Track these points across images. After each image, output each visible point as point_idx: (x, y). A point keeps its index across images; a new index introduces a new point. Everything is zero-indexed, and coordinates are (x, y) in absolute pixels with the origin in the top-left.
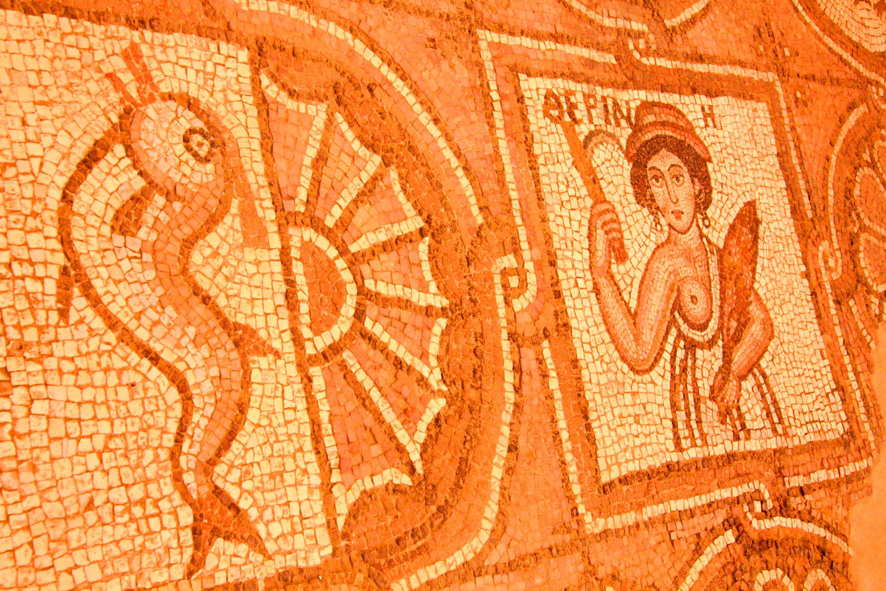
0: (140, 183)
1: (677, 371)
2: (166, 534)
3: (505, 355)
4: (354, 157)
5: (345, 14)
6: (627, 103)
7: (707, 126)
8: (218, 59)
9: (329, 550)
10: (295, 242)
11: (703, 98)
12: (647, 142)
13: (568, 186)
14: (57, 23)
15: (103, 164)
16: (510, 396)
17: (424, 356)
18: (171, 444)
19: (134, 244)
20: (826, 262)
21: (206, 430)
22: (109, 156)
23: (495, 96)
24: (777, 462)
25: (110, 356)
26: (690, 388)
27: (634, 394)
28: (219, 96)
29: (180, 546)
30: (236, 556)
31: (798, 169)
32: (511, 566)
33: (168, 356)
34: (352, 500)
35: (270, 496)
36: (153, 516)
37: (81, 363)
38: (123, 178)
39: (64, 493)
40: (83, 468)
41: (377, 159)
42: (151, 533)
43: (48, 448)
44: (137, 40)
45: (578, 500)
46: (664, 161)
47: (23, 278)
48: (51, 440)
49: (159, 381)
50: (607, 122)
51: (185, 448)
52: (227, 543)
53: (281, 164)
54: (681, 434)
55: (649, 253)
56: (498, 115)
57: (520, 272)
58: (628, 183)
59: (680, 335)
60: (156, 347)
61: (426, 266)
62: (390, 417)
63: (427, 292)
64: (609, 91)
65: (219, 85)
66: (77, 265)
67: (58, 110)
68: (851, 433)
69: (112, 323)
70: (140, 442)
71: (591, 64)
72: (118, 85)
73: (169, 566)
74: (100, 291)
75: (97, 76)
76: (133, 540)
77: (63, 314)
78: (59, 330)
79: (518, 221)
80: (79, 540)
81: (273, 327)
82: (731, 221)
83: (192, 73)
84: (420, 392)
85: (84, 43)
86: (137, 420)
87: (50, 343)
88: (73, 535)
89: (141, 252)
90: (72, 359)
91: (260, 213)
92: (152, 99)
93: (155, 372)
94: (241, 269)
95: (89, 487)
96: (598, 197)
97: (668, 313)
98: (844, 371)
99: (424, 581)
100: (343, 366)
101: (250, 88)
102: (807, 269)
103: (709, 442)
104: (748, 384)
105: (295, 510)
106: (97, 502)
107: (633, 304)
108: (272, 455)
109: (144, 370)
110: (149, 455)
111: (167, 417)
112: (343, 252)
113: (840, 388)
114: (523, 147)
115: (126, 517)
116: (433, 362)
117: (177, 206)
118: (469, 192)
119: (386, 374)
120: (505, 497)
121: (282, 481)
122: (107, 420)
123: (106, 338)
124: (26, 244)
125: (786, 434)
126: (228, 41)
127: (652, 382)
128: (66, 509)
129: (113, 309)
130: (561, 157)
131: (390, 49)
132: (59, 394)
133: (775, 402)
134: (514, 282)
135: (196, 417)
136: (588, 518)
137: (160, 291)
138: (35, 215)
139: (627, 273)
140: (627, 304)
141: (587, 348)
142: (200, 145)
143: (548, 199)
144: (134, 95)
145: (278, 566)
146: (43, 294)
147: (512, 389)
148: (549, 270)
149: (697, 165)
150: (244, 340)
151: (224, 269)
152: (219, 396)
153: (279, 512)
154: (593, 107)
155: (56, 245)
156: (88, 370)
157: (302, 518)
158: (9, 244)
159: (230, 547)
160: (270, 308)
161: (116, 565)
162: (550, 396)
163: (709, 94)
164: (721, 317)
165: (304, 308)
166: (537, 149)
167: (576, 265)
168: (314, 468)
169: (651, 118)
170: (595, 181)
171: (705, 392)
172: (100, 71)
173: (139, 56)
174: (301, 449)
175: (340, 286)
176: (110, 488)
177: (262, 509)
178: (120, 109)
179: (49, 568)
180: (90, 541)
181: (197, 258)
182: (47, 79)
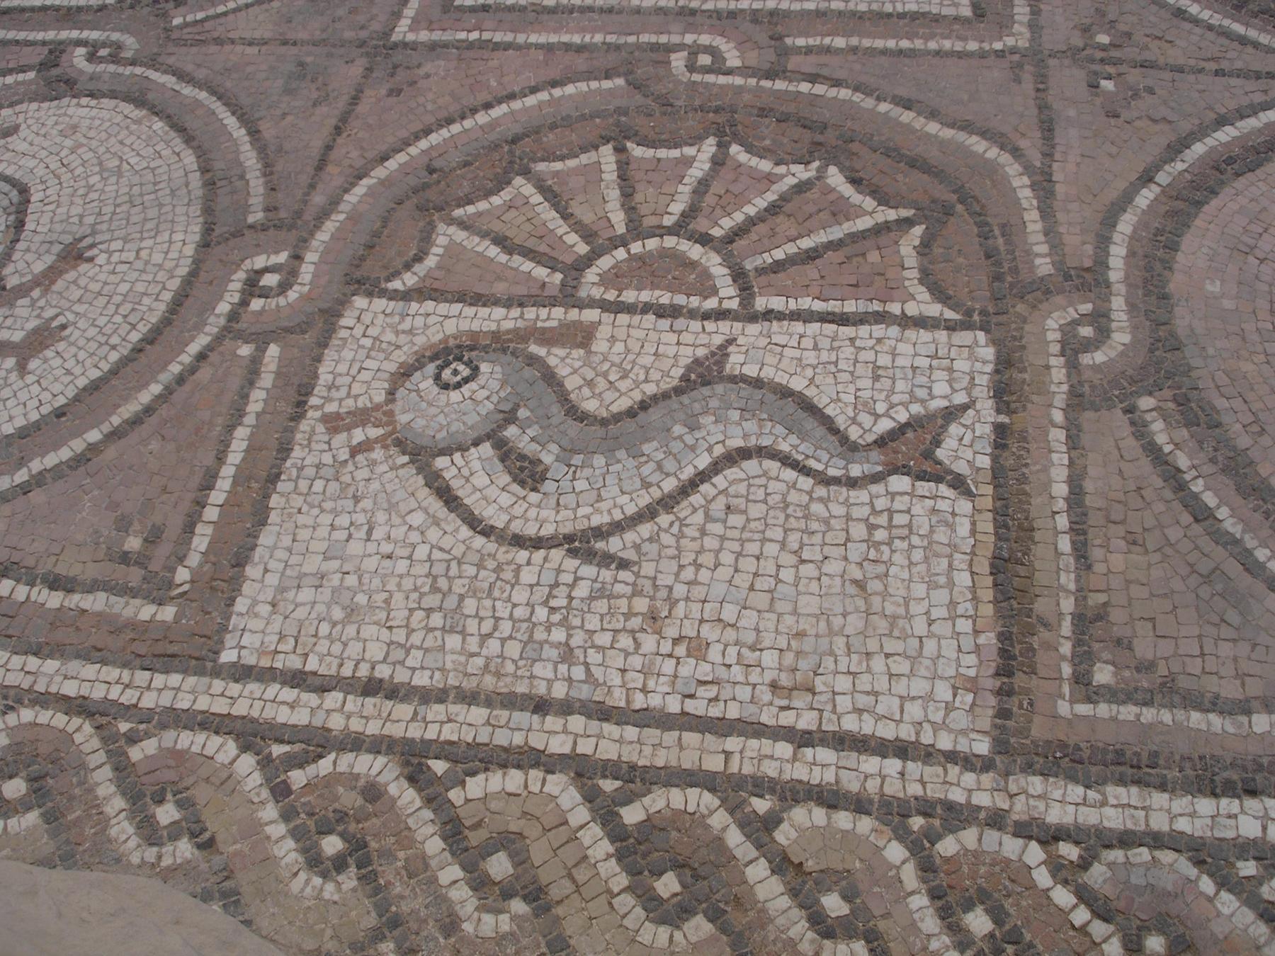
0: (486, 449)
2: (917, 510)
5: (338, 181)
8: (358, 331)
9: (981, 335)
10: (597, 293)
14: (282, 495)
15: (455, 484)
16: (844, 93)
17: (770, 179)
18: (810, 481)
19: (558, 470)
22: (447, 475)
23: (474, 36)
25: (687, 525)
28: (403, 339)
29: (935, 497)
30: (961, 439)
33: (703, 462)
34: (926, 296)
35: (900, 385)
36: (891, 519)
37: (688, 558)
38: (476, 465)
40: (815, 584)
41: (519, 181)
42: (909, 526)
43: (780, 615)
44: (318, 414)
45: (986, 46)
47: (570, 598)
49: (731, 478)
51: (820, 467)
52: (943, 445)
53: (500, 289)
56: (498, 37)
57: (695, 50)
60: (688, 473)
61: (662, 153)
62: (836, 233)
63: (694, 158)
65: (389, 336)
66: (569, 538)
67: (381, 517)
69: (648, 514)
70: (800, 515)
73: (954, 514)
74: (606, 519)
75: (350, 467)
76: (914, 547)
77: (624, 564)
78: (642, 573)
81: (697, 340)
84: (813, 194)
85: (310, 472)
86: (771, 513)
87: (655, 586)
88: (890, 609)
89: (569, 466)
90: (681, 567)
91: (554, 324)
92: (391, 414)
93: (719, 480)
94: (617, 360)
95: (838, 581)
99: (1041, 238)
100: (761, 271)
101: (401, 303)
105: (923, 362)
106: (858, 575)
108: (852, 373)
109: (713, 492)
110: (817, 508)
111: (777, 479)
112: (623, 242)
114: (545, 17)
115: (884, 548)
116: (782, 169)
117: (523, 413)
118: (583, 86)
119: (783, 224)
120: (967, 127)
122: (762, 545)
123: (665, 525)
124: (531, 586)
126: (340, 316)
128: (857, 611)
129: (631, 510)
131: (391, 139)
132: (719, 590)
134: (705, 60)
135: (784, 447)
136: (1010, 41)
137: (621, 454)
138: (498, 569)
142: (455, 372)
144: (380, 431)
145: (985, 395)
146: (595, 581)
147: (835, 89)
148: (699, 19)
150: (705, 374)
151: (612, 378)
152: (765, 416)
153: (922, 380)
155: (539, 555)
156: (698, 553)
157: (935, 356)
158: (527, 604)
159: (949, 443)
160: (673, 338)
161: (938, 571)
162: (854, 50)
165: (680, 300)
168: (878, 330)
172: (346, 461)
174: (852, 340)
175: (664, 253)
176: (846, 559)
177: (913, 399)
178: (393, 450)
179: (921, 641)
180: (903, 592)
181: (591, 406)
182: (344, 520)
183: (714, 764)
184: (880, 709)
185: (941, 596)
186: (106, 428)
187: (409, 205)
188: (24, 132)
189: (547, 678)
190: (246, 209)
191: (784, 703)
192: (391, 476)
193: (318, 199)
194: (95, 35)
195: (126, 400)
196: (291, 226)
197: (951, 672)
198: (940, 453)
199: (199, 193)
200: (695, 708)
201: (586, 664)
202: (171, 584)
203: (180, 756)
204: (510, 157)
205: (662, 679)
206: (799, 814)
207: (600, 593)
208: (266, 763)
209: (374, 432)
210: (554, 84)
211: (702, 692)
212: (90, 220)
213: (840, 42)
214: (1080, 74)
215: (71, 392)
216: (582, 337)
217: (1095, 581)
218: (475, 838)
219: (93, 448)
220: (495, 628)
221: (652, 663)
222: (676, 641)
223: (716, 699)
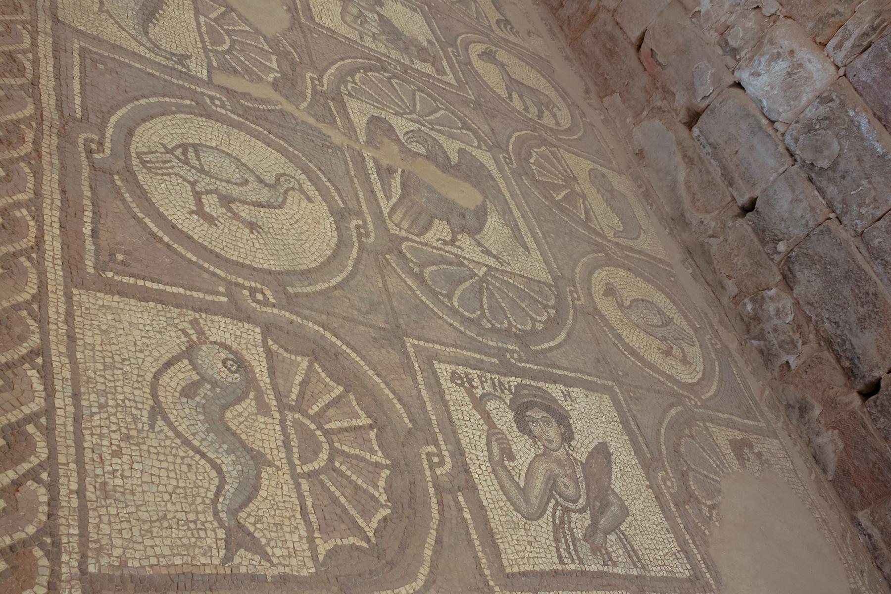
0: (196, 377)
2: (209, 541)
4: (326, 385)
6: (509, 383)
7: (566, 400)
8: (242, 329)
11: (562, 387)
17: (376, 486)
18: (212, 497)
19: (193, 403)
21: (233, 494)
23: (417, 369)
28: (244, 346)
29: (218, 548)
33: (211, 455)
35: (274, 535)
39: (149, 509)
41: (341, 388)
42: (200, 537)
46: (537, 414)
47: (131, 407)
48: (143, 482)
50: (495, 390)
51: (221, 500)
55: (531, 459)
64: (496, 376)
65: (243, 341)
66: (160, 406)
69: (178, 435)
71: (482, 361)
72: (186, 334)
73: (211, 556)
74: (173, 420)
77: (152, 426)
79: (437, 430)
80: (158, 533)
83: (228, 335)
87: (143, 438)
88: (155, 530)
90: (156, 447)
92: (205, 343)
93: (203, 462)
103: (585, 562)
106: (169, 517)
110: (199, 500)
111: (210, 484)
115: (185, 527)
116: (382, 491)
121: (282, 528)
128: (151, 517)
129: (180, 429)
130: (464, 403)
131: (348, 339)
134: (436, 460)
137: (206, 425)
138: (138, 382)
139: (516, 467)
142: (232, 365)
143: (457, 422)
144: (195, 339)
149: (562, 419)
150: (258, 459)
153: (280, 544)
154: (486, 382)
159: (249, 556)
160: (273, 445)
166: (447, 397)
168: (302, 527)
169: (526, 392)
170: (489, 417)
171: (579, 534)
173: (198, 324)
174: (294, 516)
176: (176, 511)
181: (229, 415)
182: (148, 328)
183: (61, 459)
184: (102, 526)
185: (167, 551)
186: (171, 243)
187: (314, 346)
188: (310, 205)
189: (89, 400)
190: (293, 286)
191: (97, 486)
192: (174, 343)
193: (307, 312)
194: (371, 227)
195: (186, 249)
196: (290, 302)
197: (128, 556)
199: (297, 269)
200: (88, 453)
201: (100, 413)
202: (104, 271)
203: (25, 273)
204: (350, 381)
205: (99, 441)
206: (43, 490)
207: (135, 419)
208: (28, 303)
209: (194, 337)
210: (400, 400)
211: (96, 457)
212: (271, 231)
215: (185, 230)
216: (263, 409)
218: (9, 373)
219: (160, 240)
220: (110, 381)
221: (107, 437)
222: (119, 446)
223: (94, 461)
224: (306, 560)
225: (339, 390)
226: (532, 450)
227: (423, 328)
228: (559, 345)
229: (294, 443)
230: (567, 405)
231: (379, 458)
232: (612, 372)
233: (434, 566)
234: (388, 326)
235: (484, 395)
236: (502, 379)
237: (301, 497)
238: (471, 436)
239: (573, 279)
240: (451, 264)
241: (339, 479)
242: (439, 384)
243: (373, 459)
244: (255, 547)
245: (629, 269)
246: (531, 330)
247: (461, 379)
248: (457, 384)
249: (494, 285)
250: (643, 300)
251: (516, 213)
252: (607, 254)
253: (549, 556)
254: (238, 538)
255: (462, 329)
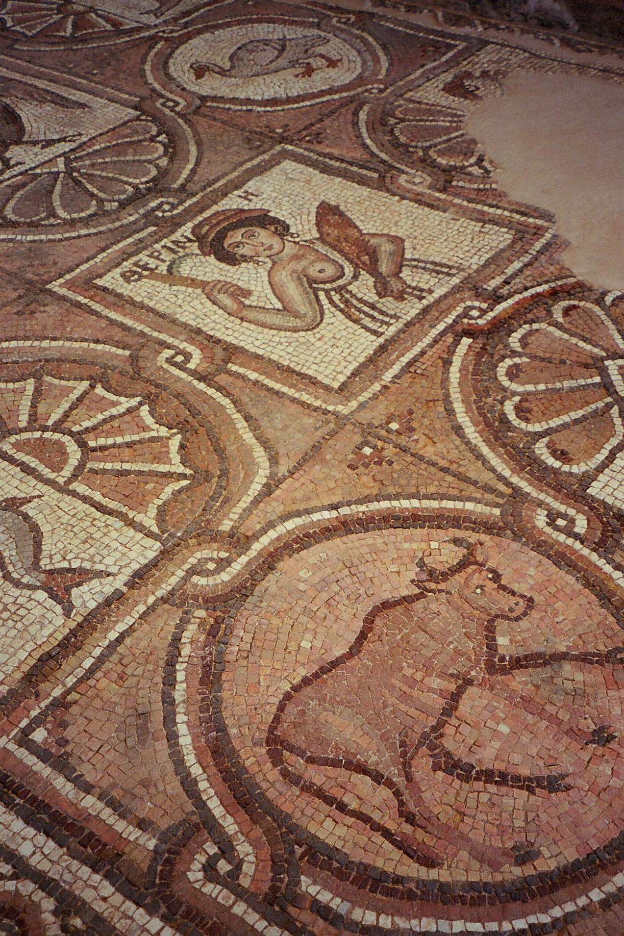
1: (342, 306)
3: (205, 390)
7: (250, 200)
11: (237, 193)
12: (213, 239)
13: (176, 296)
20: (414, 183)
23: (85, 301)
24: (473, 285)
26: (360, 306)
27: (319, 339)
31: (343, 165)
32: (299, 466)
41: (32, 381)
42: (23, 617)
46: (237, 236)
50: (175, 252)
54: (375, 328)
58: (218, 263)
59: (327, 292)
64: (165, 240)
68: (519, 231)
71: (140, 241)
73: (50, 622)
79: (155, 334)
82: (314, 222)
96: (203, 285)
97: (309, 289)
98: (483, 213)
102: (399, 195)
104: (405, 273)
107: (279, 305)
113: (483, 219)
125: (460, 269)
127: (329, 324)
130: (158, 290)
133: (436, 264)
134: (180, 358)
136: (340, 408)
140: (274, 309)
141: (264, 346)
143: (168, 311)
149: (263, 220)
153: (105, 552)
154: (161, 254)
159: (84, 588)
160: (15, 482)
163: (237, 188)
164: (351, 261)
167: (217, 321)
168: (111, 520)
169: (207, 228)
170: (193, 280)
174: (95, 519)
175: (58, 443)
198: (75, 591)
210: (97, 342)
213: (253, 376)
214: (358, 439)
217: (82, 688)
224: (143, 542)
225: (30, 385)
226: (260, 270)
227: (55, 263)
228: (198, 163)
229: (34, 463)
230: (255, 204)
231: (126, 403)
232: (267, 137)
233: (263, 442)
234: (21, 292)
235: (170, 269)
236: (173, 237)
237: (85, 499)
238: (192, 310)
239: (154, 90)
240: (24, 185)
241: (107, 453)
242: (120, 296)
243: (122, 409)
244: (82, 576)
245: (199, 32)
246: (159, 173)
247: (135, 273)
248: (136, 280)
249: (84, 166)
250: (239, 48)
251: (41, 84)
252: (166, 40)
253: (362, 340)
254: (60, 584)
255: (93, 231)
